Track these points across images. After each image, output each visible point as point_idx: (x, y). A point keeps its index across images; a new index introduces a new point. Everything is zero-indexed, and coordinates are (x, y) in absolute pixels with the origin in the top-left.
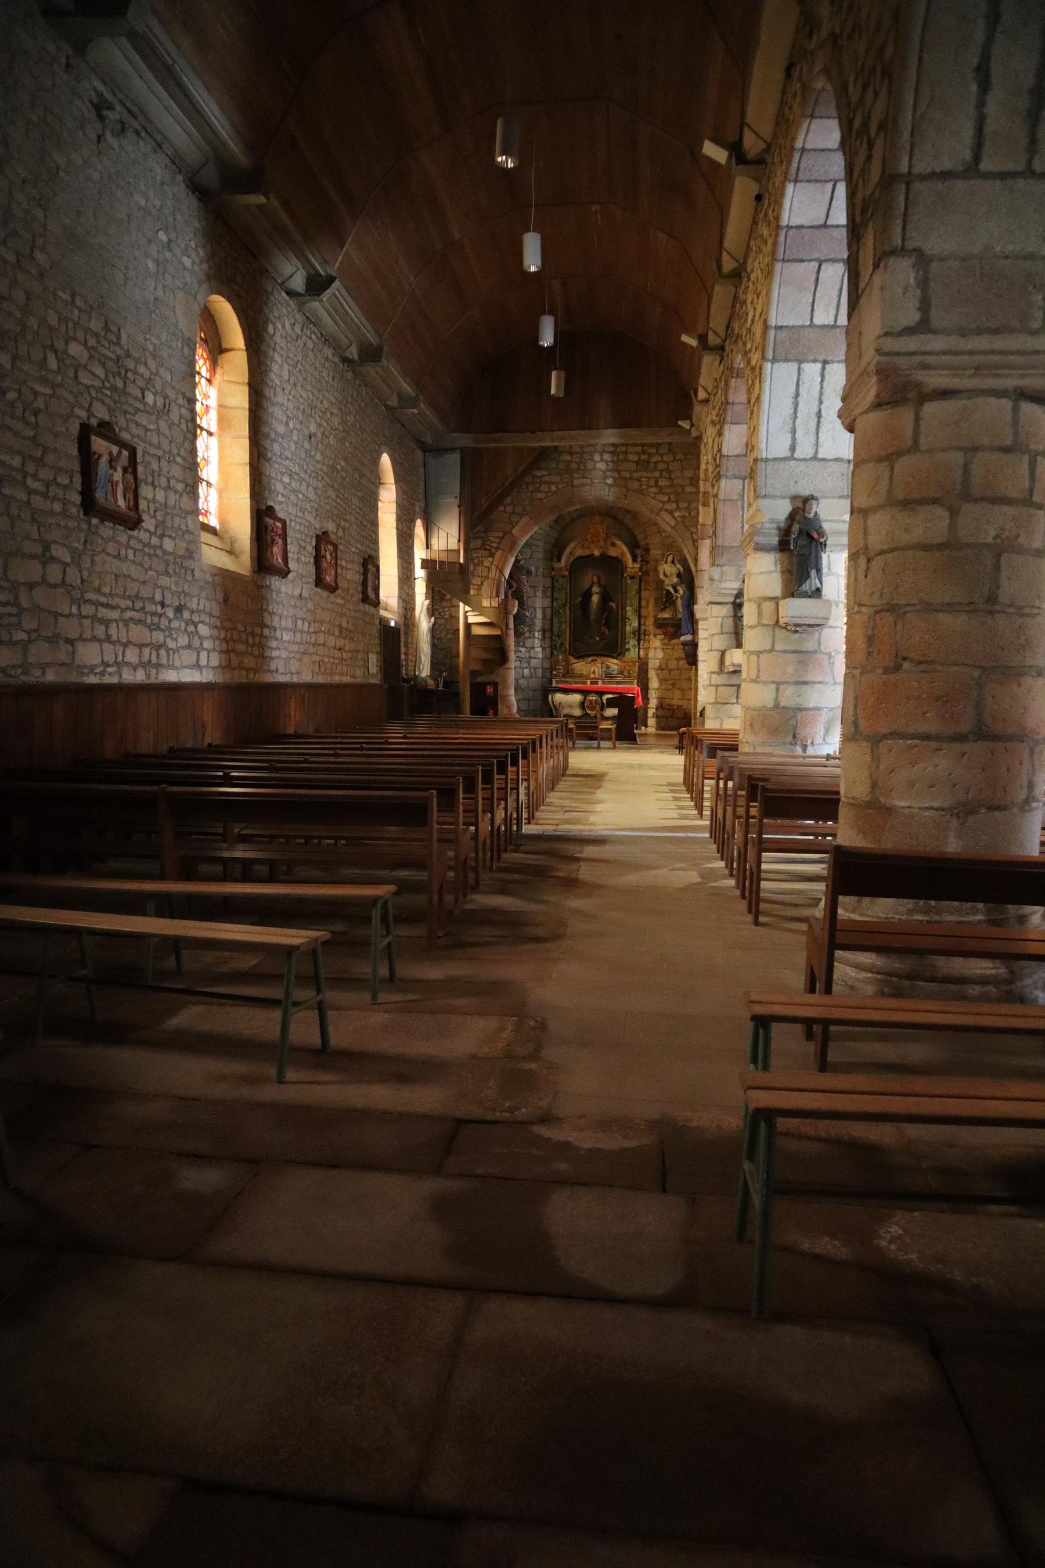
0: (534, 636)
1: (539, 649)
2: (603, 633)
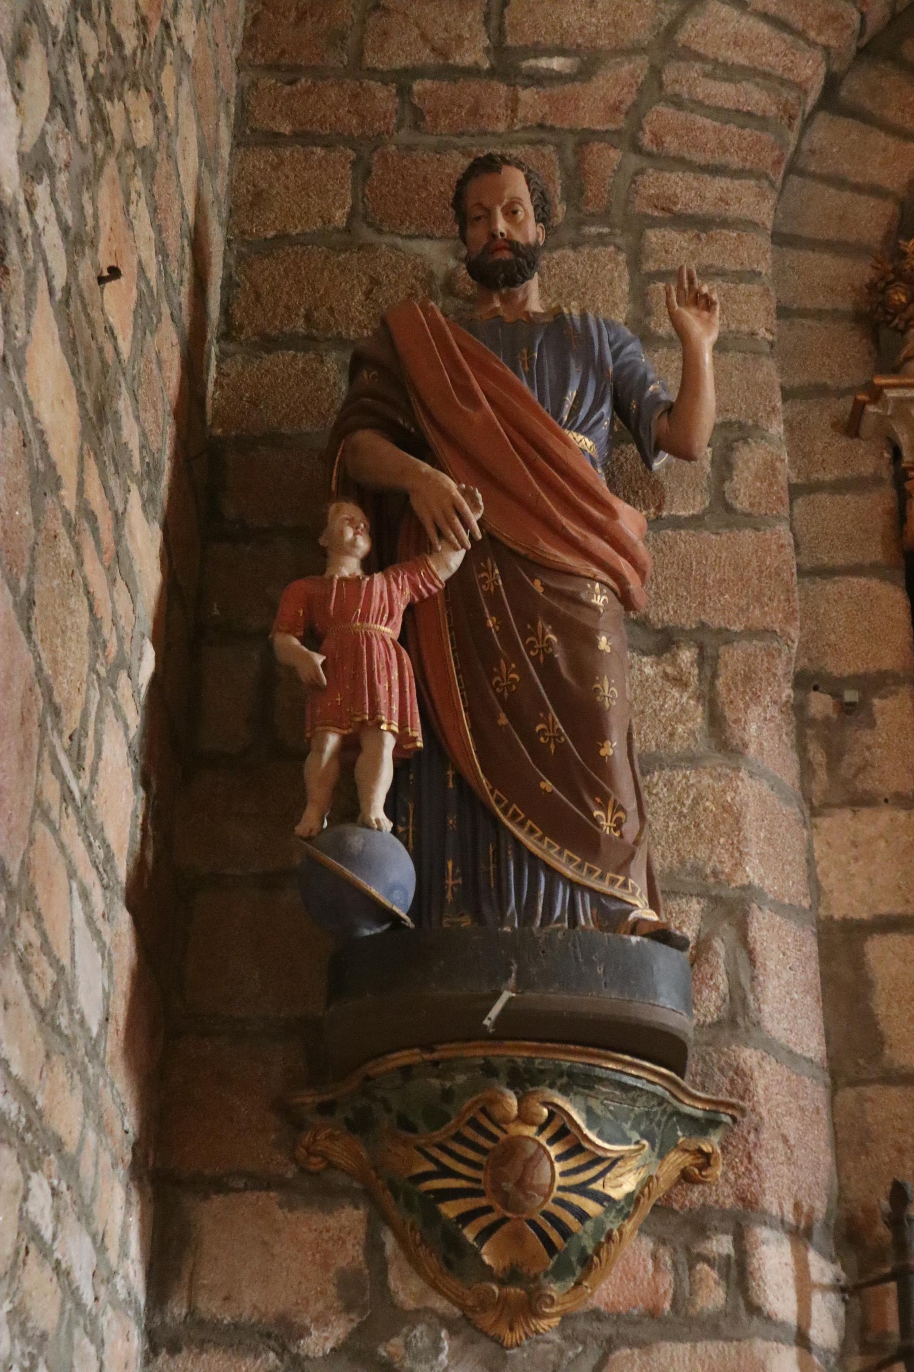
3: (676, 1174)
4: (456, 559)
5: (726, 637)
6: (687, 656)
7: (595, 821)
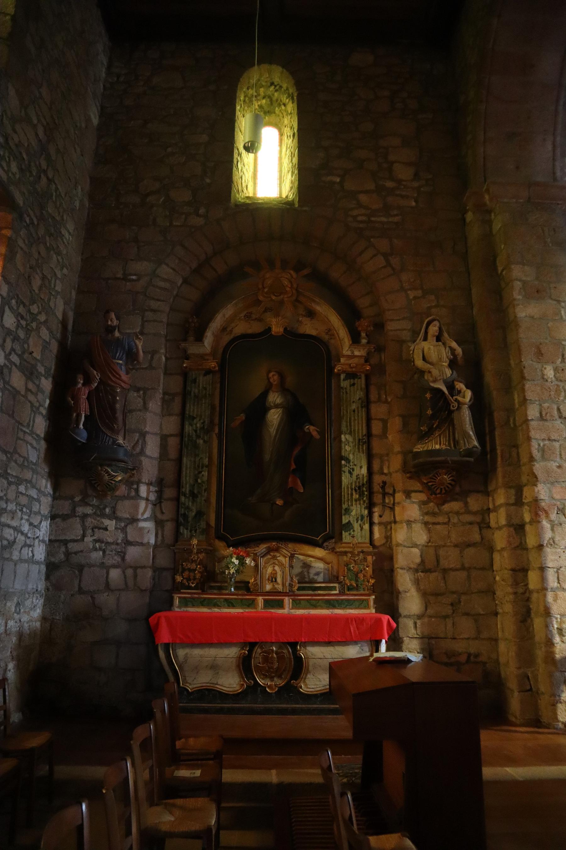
0: (138, 496)
1: (149, 525)
4: (96, 384)
5: (148, 389)
6: (141, 392)
7: (114, 427)
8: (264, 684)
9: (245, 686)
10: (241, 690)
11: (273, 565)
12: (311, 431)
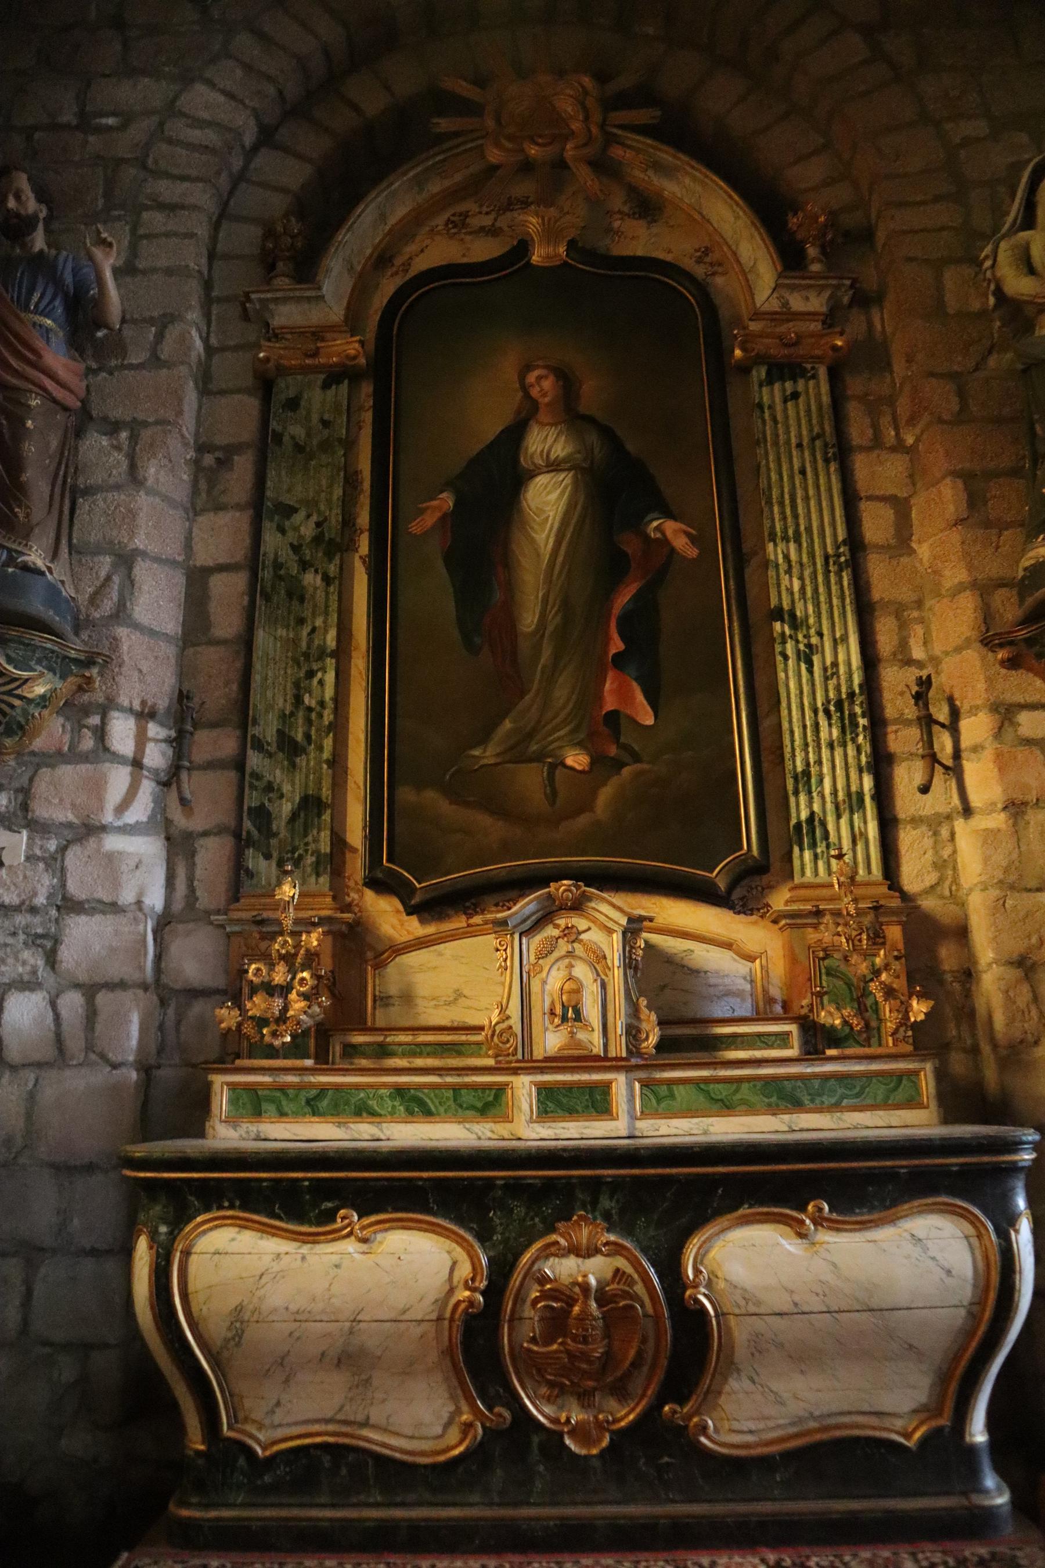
2: (613, 719)
3: (74, 688)
5: (145, 424)
6: (124, 435)
7: (16, 515)
8: (555, 1421)
9: (480, 1430)
10: (461, 1449)
11: (567, 961)
12: (669, 534)
